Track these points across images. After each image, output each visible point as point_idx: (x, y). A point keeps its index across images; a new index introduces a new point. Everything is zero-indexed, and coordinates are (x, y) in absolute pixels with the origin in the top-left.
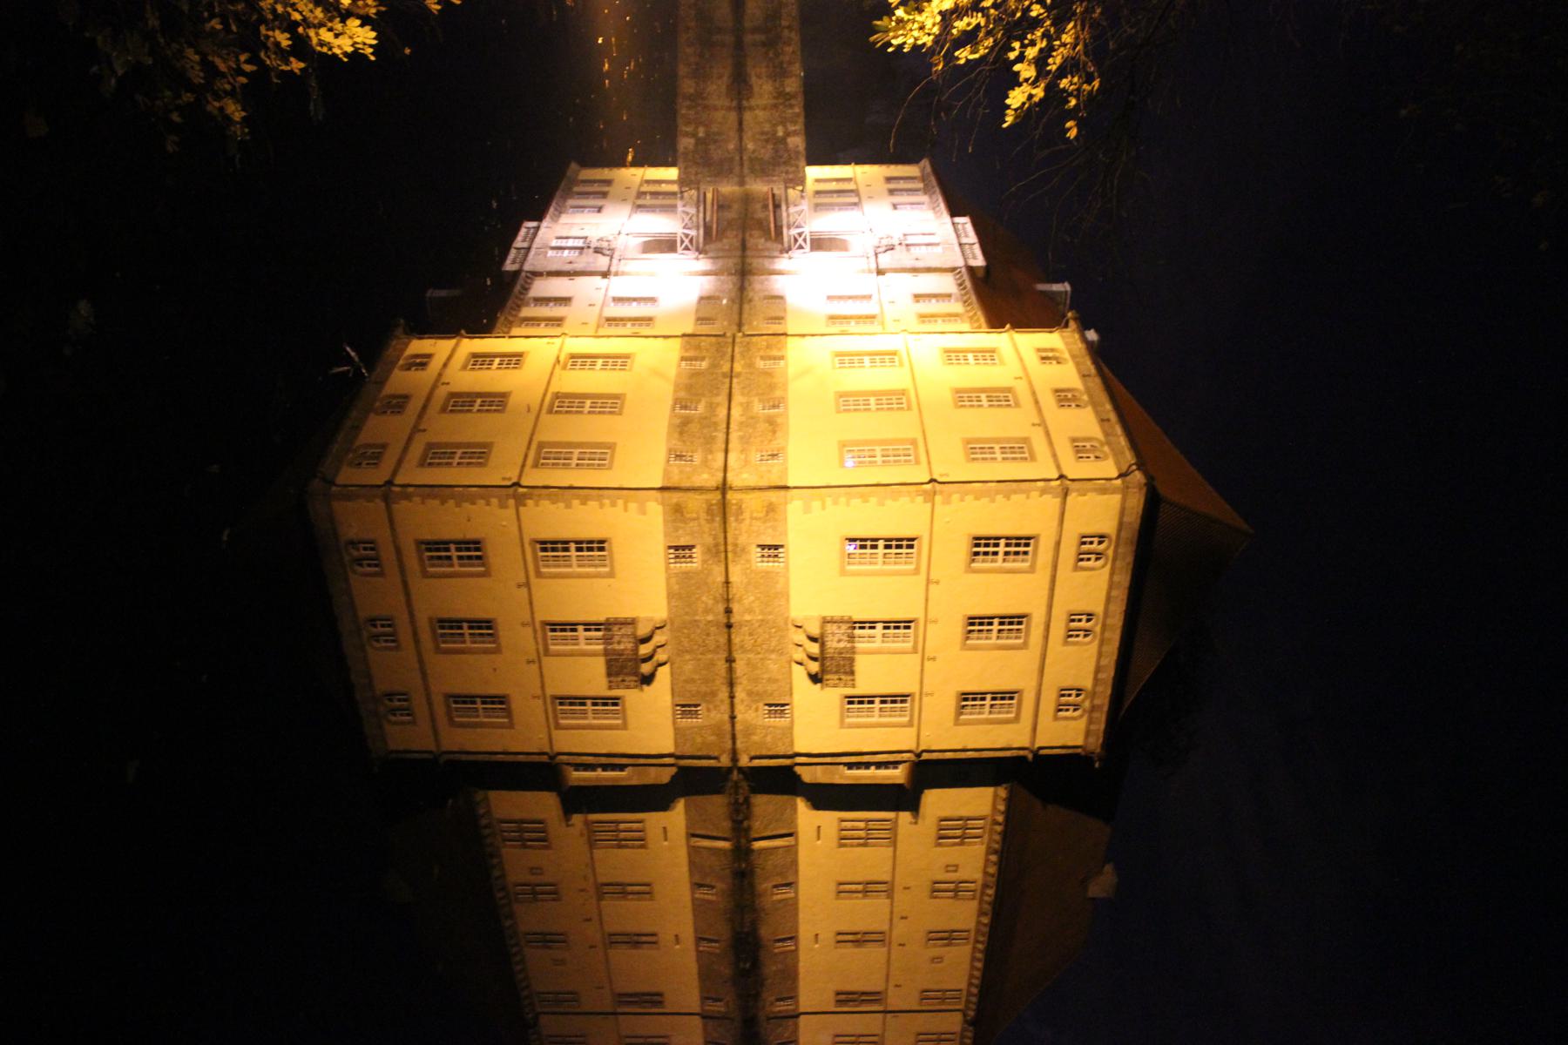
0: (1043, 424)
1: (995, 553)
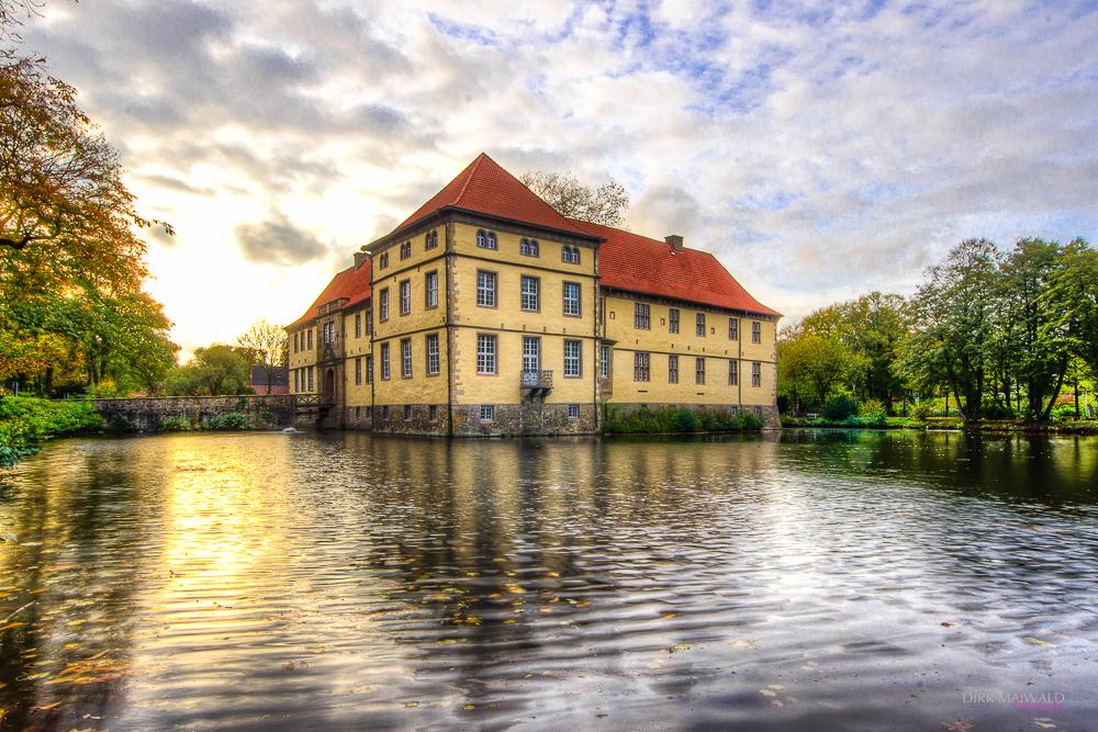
0: (418, 266)
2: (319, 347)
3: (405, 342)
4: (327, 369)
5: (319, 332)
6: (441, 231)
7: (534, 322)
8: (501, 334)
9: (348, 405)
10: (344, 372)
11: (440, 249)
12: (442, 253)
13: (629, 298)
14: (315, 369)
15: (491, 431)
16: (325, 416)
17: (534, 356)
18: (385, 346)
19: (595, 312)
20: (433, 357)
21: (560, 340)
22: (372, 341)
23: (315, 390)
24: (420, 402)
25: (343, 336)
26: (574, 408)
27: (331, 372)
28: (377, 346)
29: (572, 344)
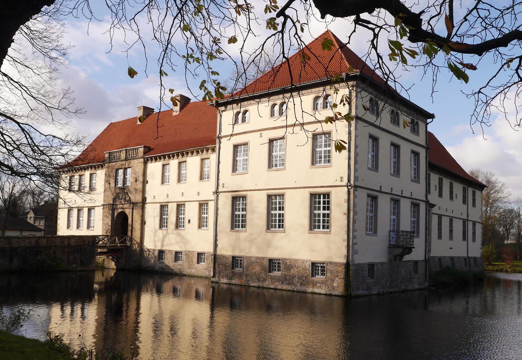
5: (107, 176)
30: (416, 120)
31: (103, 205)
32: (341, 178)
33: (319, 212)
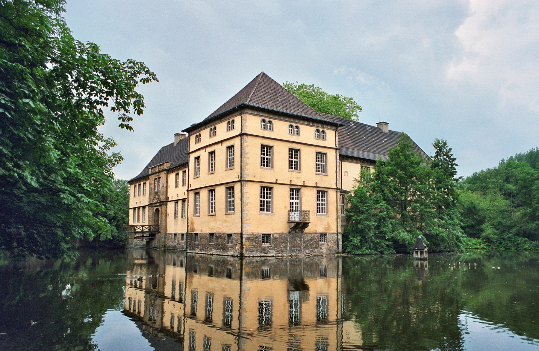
0: (221, 142)
1: (267, 159)
2: (150, 194)
3: (212, 190)
4: (155, 208)
5: (150, 184)
6: (237, 119)
7: (297, 178)
8: (276, 187)
9: (168, 232)
10: (166, 210)
11: (237, 131)
12: (238, 134)
13: (357, 163)
14: (147, 208)
15: (269, 252)
16: (153, 239)
17: (297, 201)
18: (197, 194)
19: (336, 171)
20: (230, 202)
21: (314, 191)
22: (188, 191)
23: (147, 223)
24: (220, 231)
25: (167, 187)
26: (323, 236)
27: (157, 210)
28: (192, 195)
29: (321, 193)
30: (321, 130)
31: (149, 204)
32: (238, 175)
33: (323, 202)
